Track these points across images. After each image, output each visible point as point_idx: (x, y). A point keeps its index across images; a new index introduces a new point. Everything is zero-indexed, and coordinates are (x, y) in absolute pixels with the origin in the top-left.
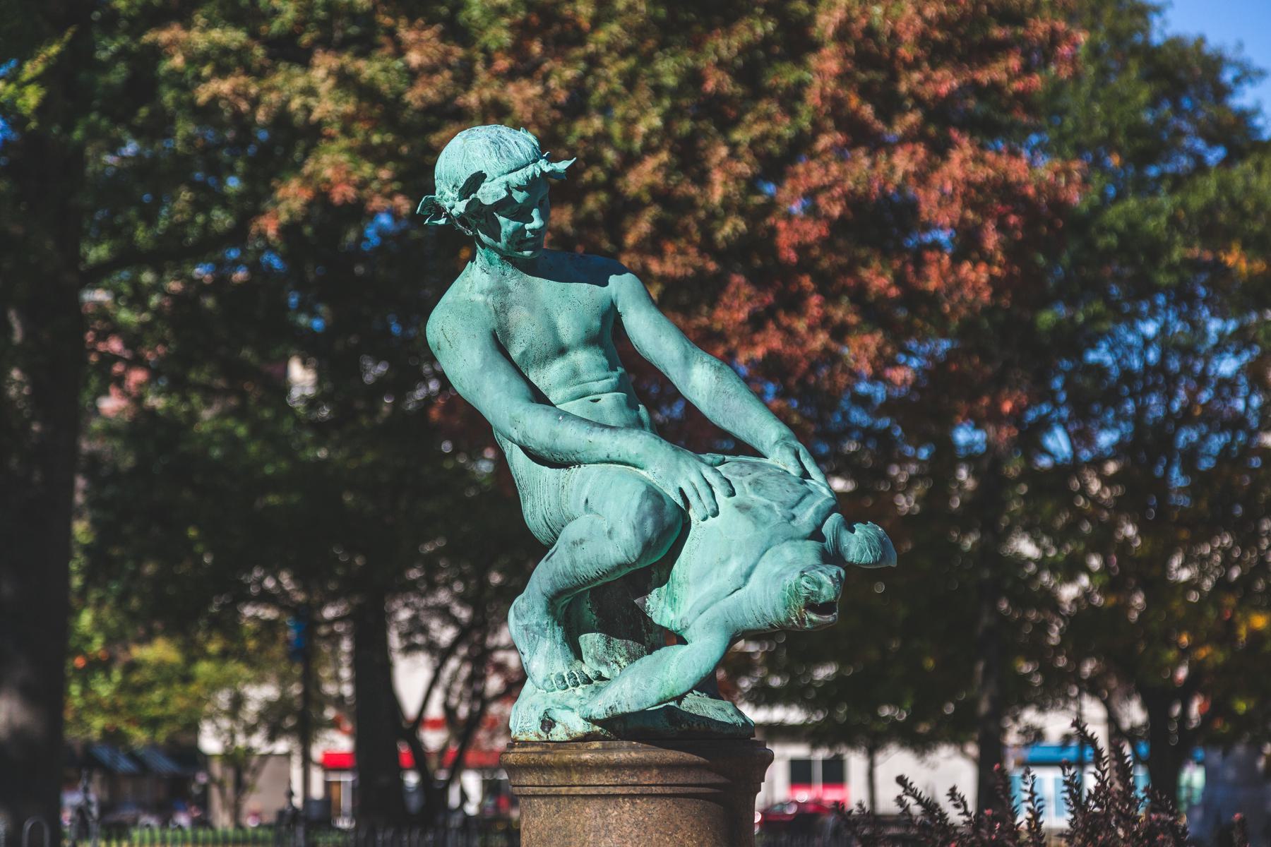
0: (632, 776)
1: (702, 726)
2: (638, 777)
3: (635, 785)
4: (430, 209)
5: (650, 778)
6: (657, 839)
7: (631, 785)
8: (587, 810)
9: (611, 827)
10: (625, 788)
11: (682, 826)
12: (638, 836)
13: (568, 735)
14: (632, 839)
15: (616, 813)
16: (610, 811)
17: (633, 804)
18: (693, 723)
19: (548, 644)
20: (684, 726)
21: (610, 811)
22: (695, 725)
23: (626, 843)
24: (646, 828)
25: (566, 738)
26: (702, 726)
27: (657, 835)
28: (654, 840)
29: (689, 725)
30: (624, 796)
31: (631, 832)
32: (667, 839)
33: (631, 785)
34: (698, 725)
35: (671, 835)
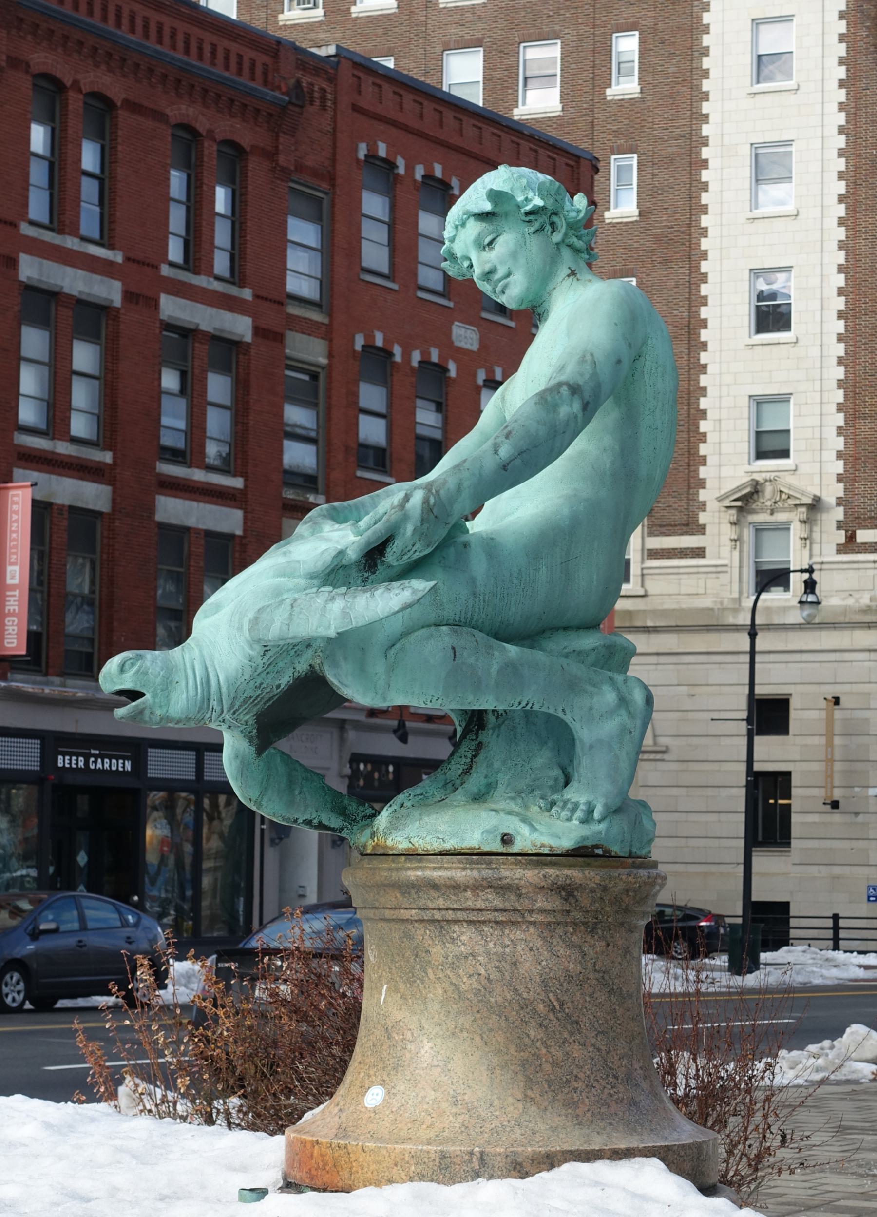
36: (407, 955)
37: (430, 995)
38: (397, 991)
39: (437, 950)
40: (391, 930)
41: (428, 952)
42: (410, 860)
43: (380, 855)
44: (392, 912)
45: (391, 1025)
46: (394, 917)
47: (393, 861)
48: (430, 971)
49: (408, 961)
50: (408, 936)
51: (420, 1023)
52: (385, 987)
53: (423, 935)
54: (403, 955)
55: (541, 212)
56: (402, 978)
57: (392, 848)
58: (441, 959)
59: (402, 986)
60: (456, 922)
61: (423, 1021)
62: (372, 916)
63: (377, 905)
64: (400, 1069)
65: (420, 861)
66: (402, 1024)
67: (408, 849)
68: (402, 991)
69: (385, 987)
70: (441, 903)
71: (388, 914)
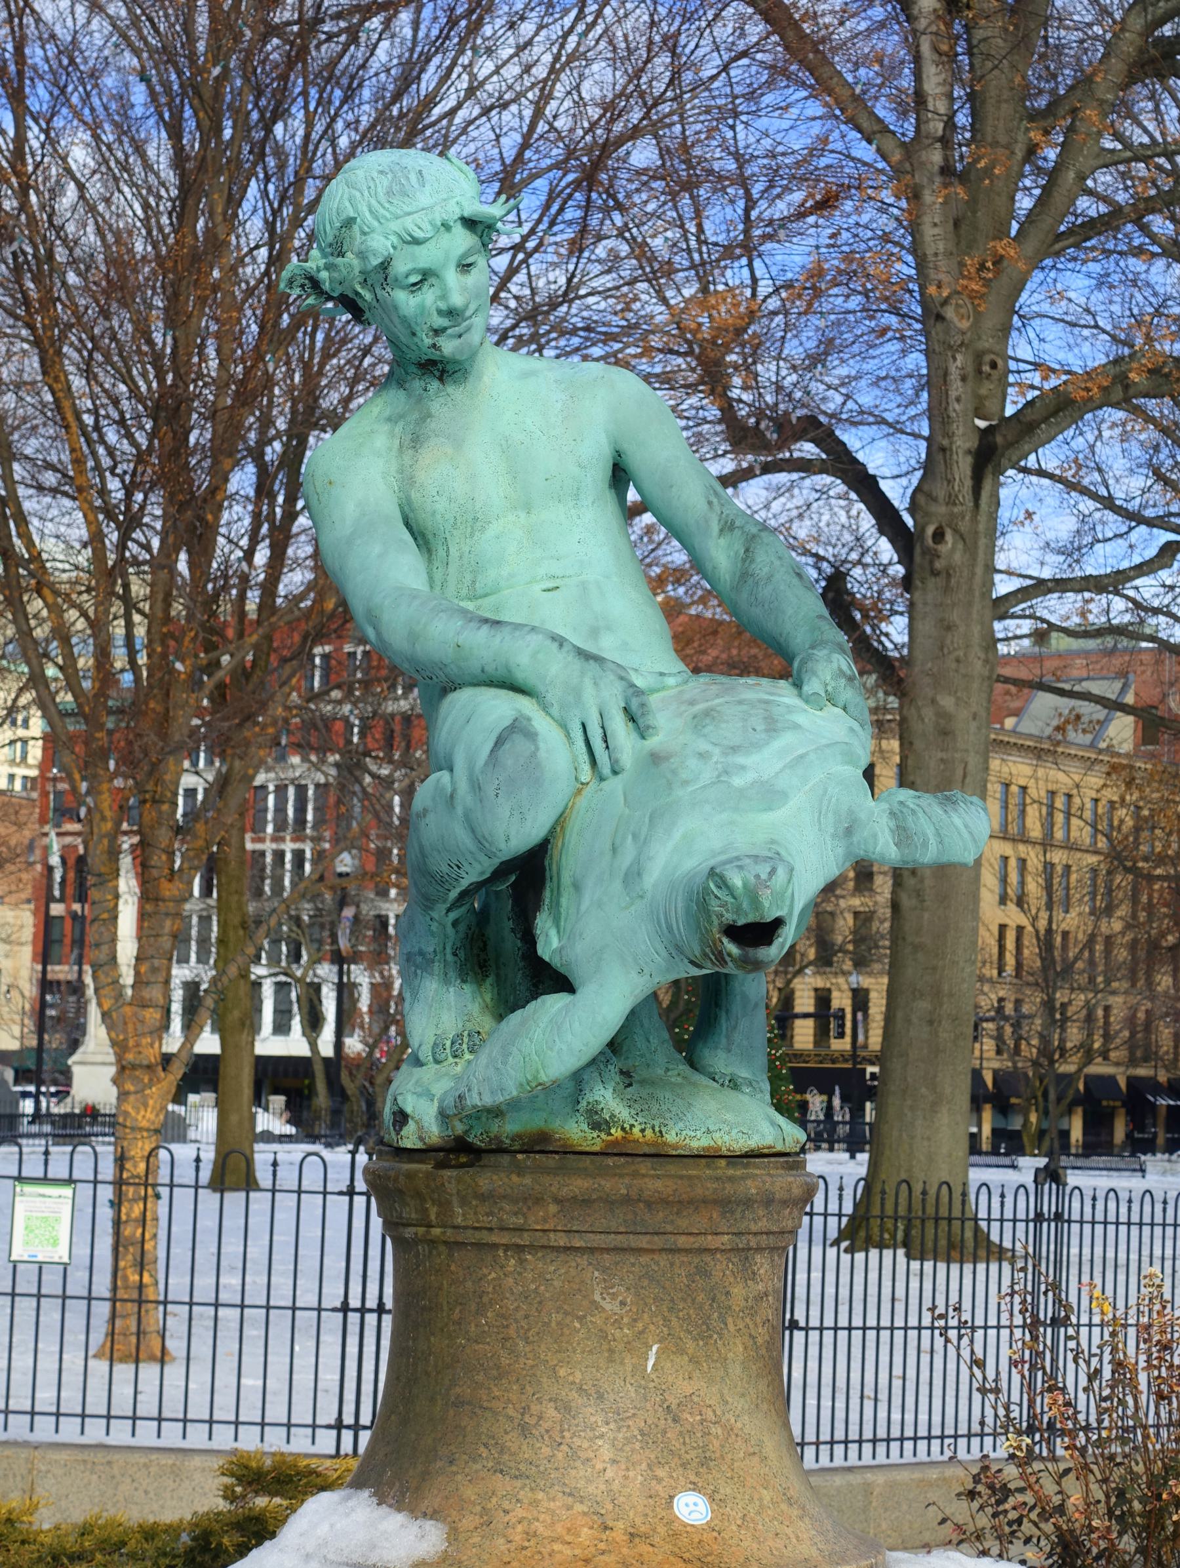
0: (516, 1214)
1: (649, 1132)
2: (524, 1214)
3: (519, 1230)
4: (302, 286)
5: (545, 1220)
6: (558, 1323)
7: (514, 1229)
8: (453, 1268)
9: (485, 1299)
10: (505, 1233)
11: (603, 1303)
12: (526, 1317)
13: (421, 1139)
14: (517, 1321)
15: (493, 1275)
16: (485, 1271)
17: (521, 1261)
18: (632, 1126)
19: (434, 985)
20: (617, 1133)
21: (485, 1271)
22: (636, 1130)
23: (507, 1326)
24: (540, 1303)
25: (419, 1145)
26: (649, 1132)
27: (560, 1317)
28: (553, 1324)
29: (623, 1129)
30: (507, 1247)
31: (517, 1309)
32: (577, 1325)
33: (514, 1229)
34: (643, 1131)
35: (584, 1317)
36: (699, 1299)
37: (730, 1355)
38: (682, 1351)
39: (738, 1291)
40: (672, 1264)
41: (728, 1293)
42: (734, 1165)
43: (645, 1155)
44: (692, 1239)
45: (675, 1402)
46: (696, 1245)
47: (708, 1166)
48: (730, 1320)
49: (701, 1308)
50: (705, 1273)
51: (722, 1395)
52: (655, 1348)
53: (721, 1268)
54: (693, 1300)
55: (480, 228)
56: (690, 1332)
57: (675, 1147)
58: (743, 1303)
59: (690, 1345)
60: (759, 1249)
61: (726, 1392)
62: (645, 1246)
63: (669, 1228)
64: (712, 1464)
65: (746, 1166)
66: (695, 1399)
67: (709, 1148)
68: (690, 1352)
69: (655, 1348)
70: (763, 1224)
71: (682, 1241)
